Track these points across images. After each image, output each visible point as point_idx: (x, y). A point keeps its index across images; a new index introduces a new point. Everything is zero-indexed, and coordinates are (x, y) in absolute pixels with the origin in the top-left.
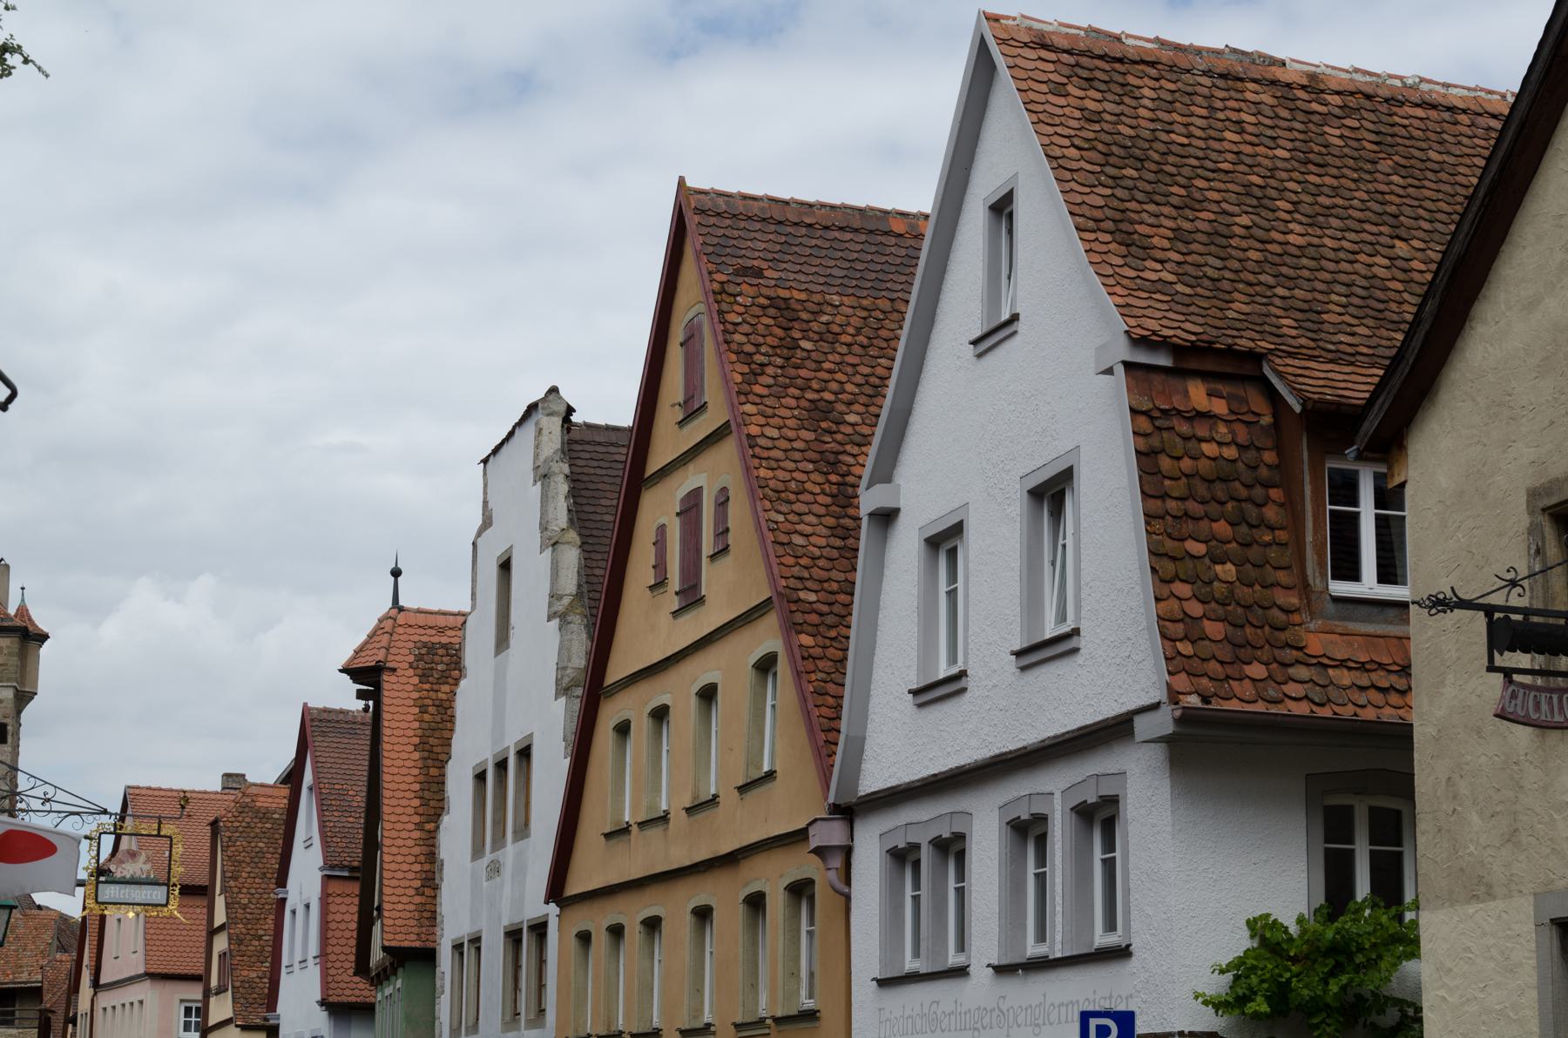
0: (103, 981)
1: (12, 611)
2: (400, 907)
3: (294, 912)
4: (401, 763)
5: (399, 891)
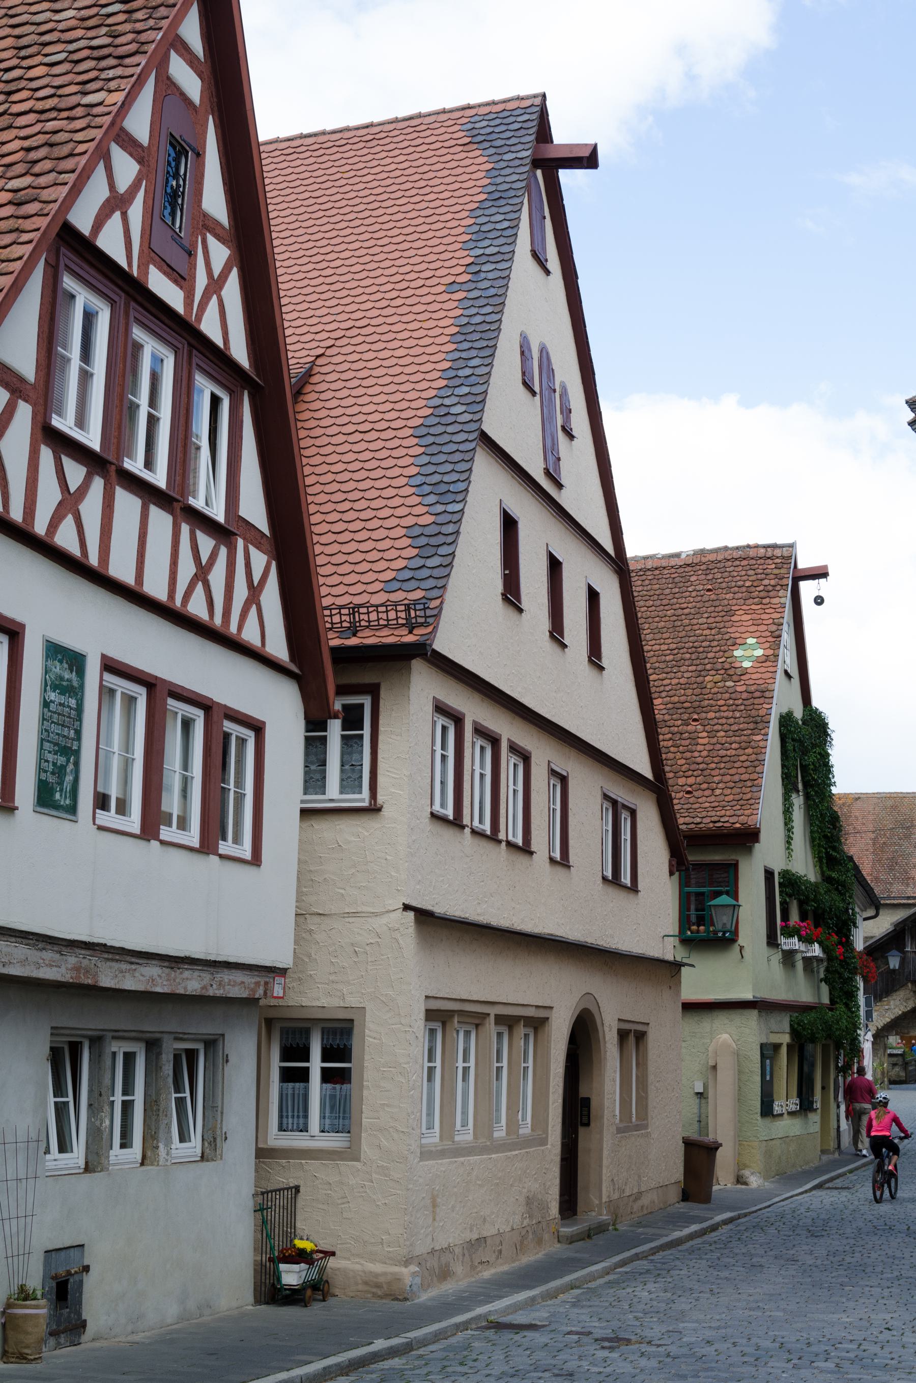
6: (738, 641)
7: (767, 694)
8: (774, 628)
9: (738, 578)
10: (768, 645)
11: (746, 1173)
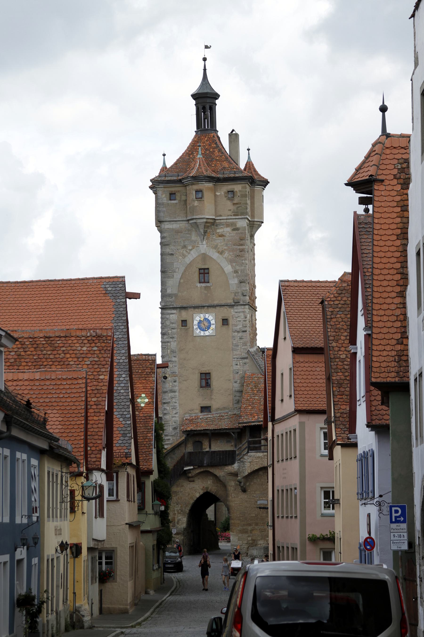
0: (276, 418)
1: (242, 166)
2: (385, 353)
3: (360, 361)
4: (387, 249)
5: (384, 342)
6: (139, 395)
7: (151, 418)
8: (151, 390)
9: (136, 369)
10: (149, 397)
11: (149, 590)
